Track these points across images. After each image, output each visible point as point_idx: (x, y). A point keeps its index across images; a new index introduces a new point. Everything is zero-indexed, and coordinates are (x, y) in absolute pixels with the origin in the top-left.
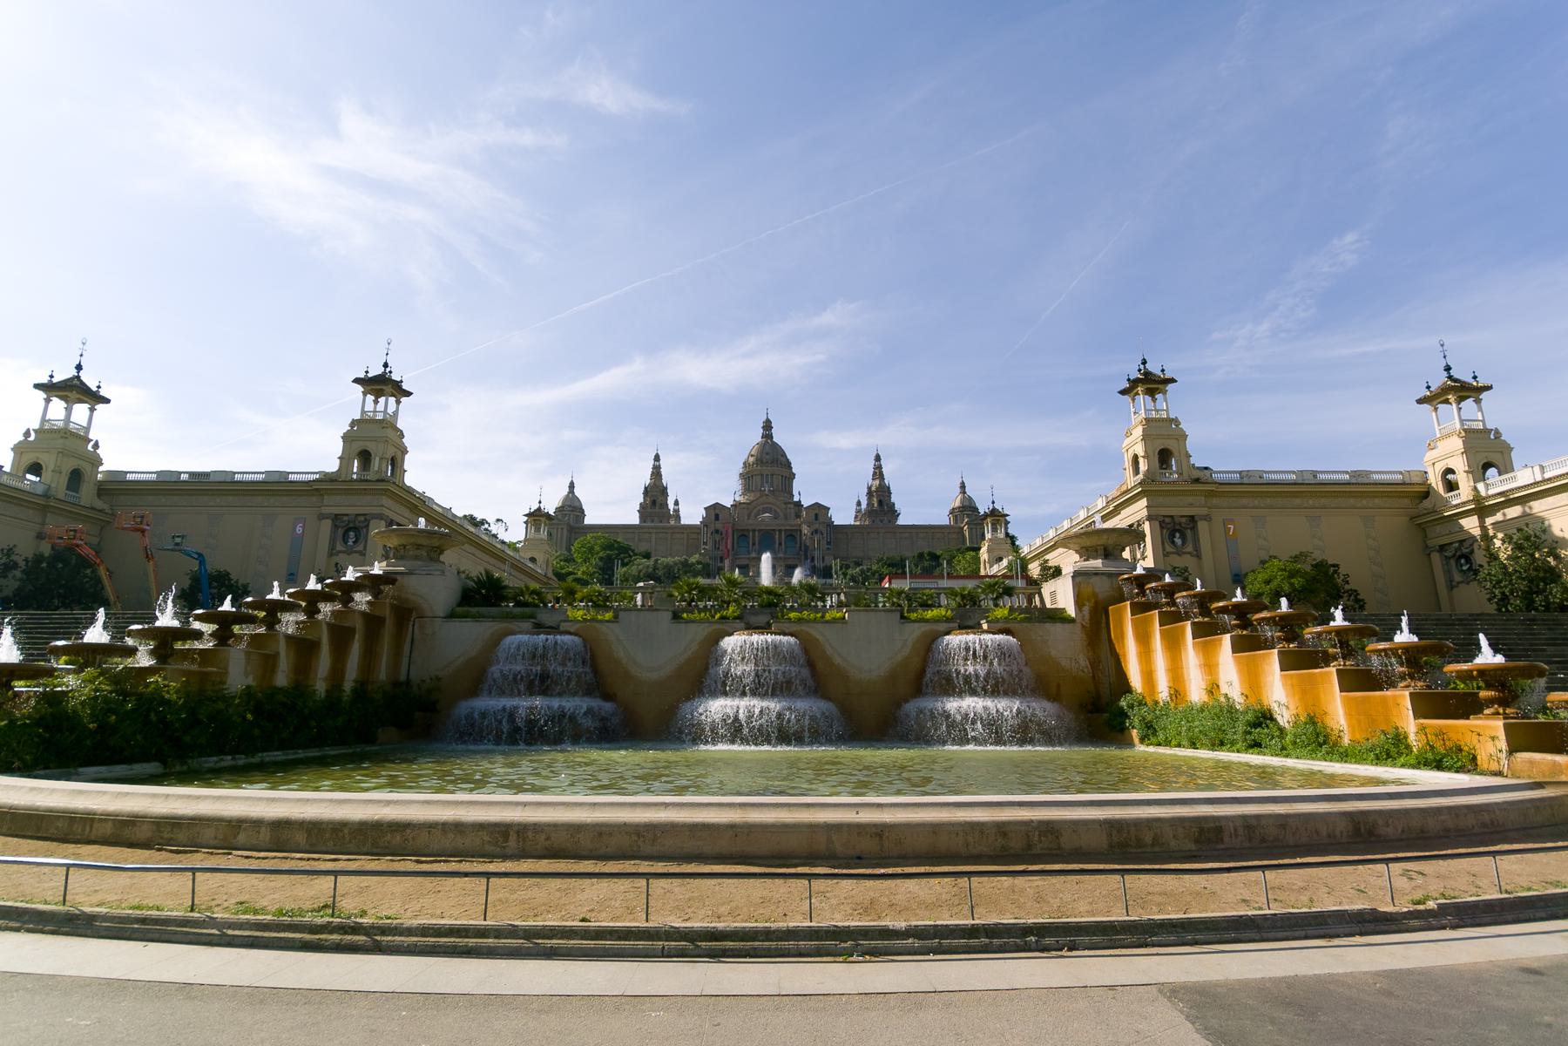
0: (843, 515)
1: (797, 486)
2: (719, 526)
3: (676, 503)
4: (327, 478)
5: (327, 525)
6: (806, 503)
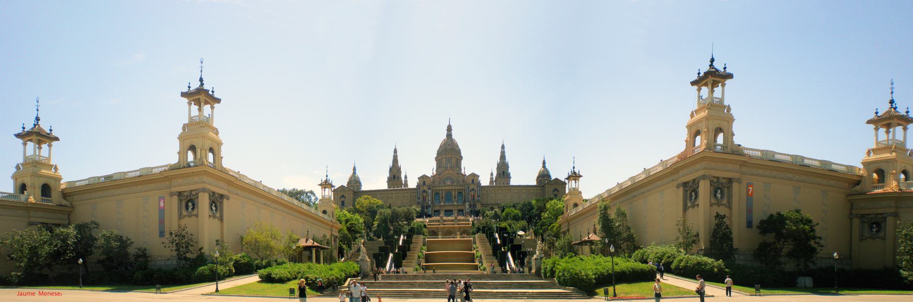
0: (485, 181)
2: (425, 188)
3: (406, 177)
4: (173, 168)
5: (175, 198)
6: (467, 174)
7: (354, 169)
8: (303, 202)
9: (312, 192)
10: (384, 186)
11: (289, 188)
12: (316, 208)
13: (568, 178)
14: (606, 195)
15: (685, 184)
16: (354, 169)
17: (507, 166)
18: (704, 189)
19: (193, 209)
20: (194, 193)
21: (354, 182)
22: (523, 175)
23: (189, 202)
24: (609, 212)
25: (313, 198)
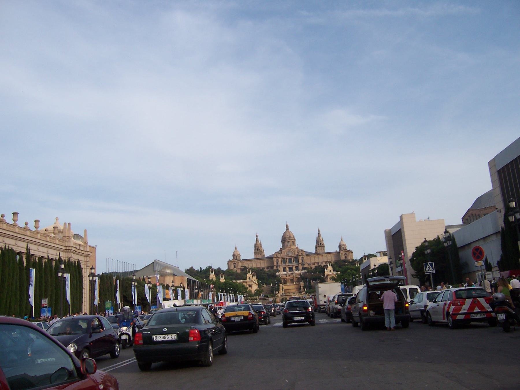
1: (297, 242)
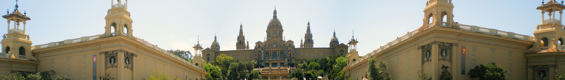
0: (297, 45)
2: (260, 49)
3: (248, 43)
4: (102, 37)
5: (103, 56)
7: (216, 38)
8: (183, 58)
9: (189, 52)
10: (234, 48)
11: (174, 50)
12: (192, 62)
13: (350, 43)
14: (373, 54)
15: (423, 47)
16: (216, 38)
17: (311, 36)
18: (435, 50)
19: (114, 62)
20: (115, 52)
21: (216, 45)
22: (321, 42)
23: (112, 58)
24: (375, 64)
25: (189, 56)
